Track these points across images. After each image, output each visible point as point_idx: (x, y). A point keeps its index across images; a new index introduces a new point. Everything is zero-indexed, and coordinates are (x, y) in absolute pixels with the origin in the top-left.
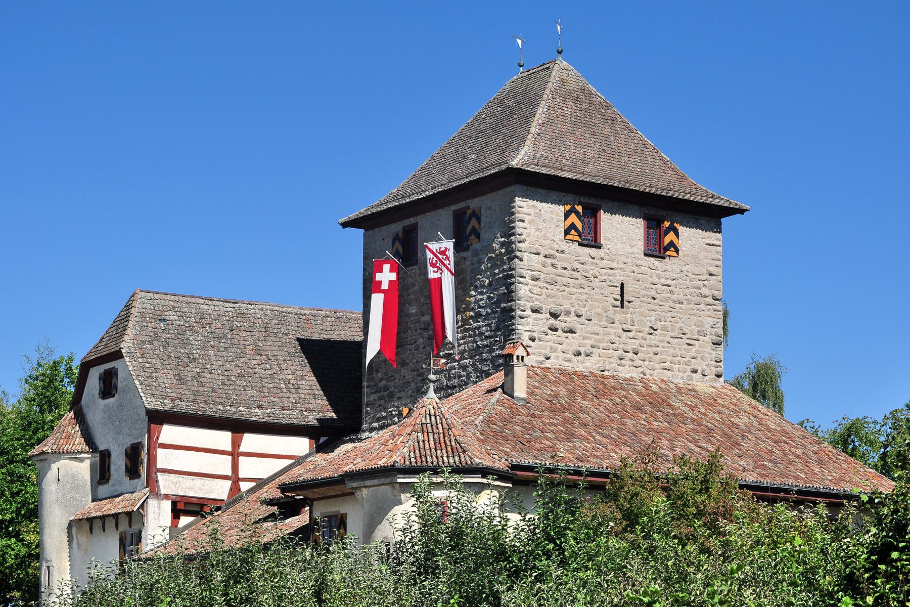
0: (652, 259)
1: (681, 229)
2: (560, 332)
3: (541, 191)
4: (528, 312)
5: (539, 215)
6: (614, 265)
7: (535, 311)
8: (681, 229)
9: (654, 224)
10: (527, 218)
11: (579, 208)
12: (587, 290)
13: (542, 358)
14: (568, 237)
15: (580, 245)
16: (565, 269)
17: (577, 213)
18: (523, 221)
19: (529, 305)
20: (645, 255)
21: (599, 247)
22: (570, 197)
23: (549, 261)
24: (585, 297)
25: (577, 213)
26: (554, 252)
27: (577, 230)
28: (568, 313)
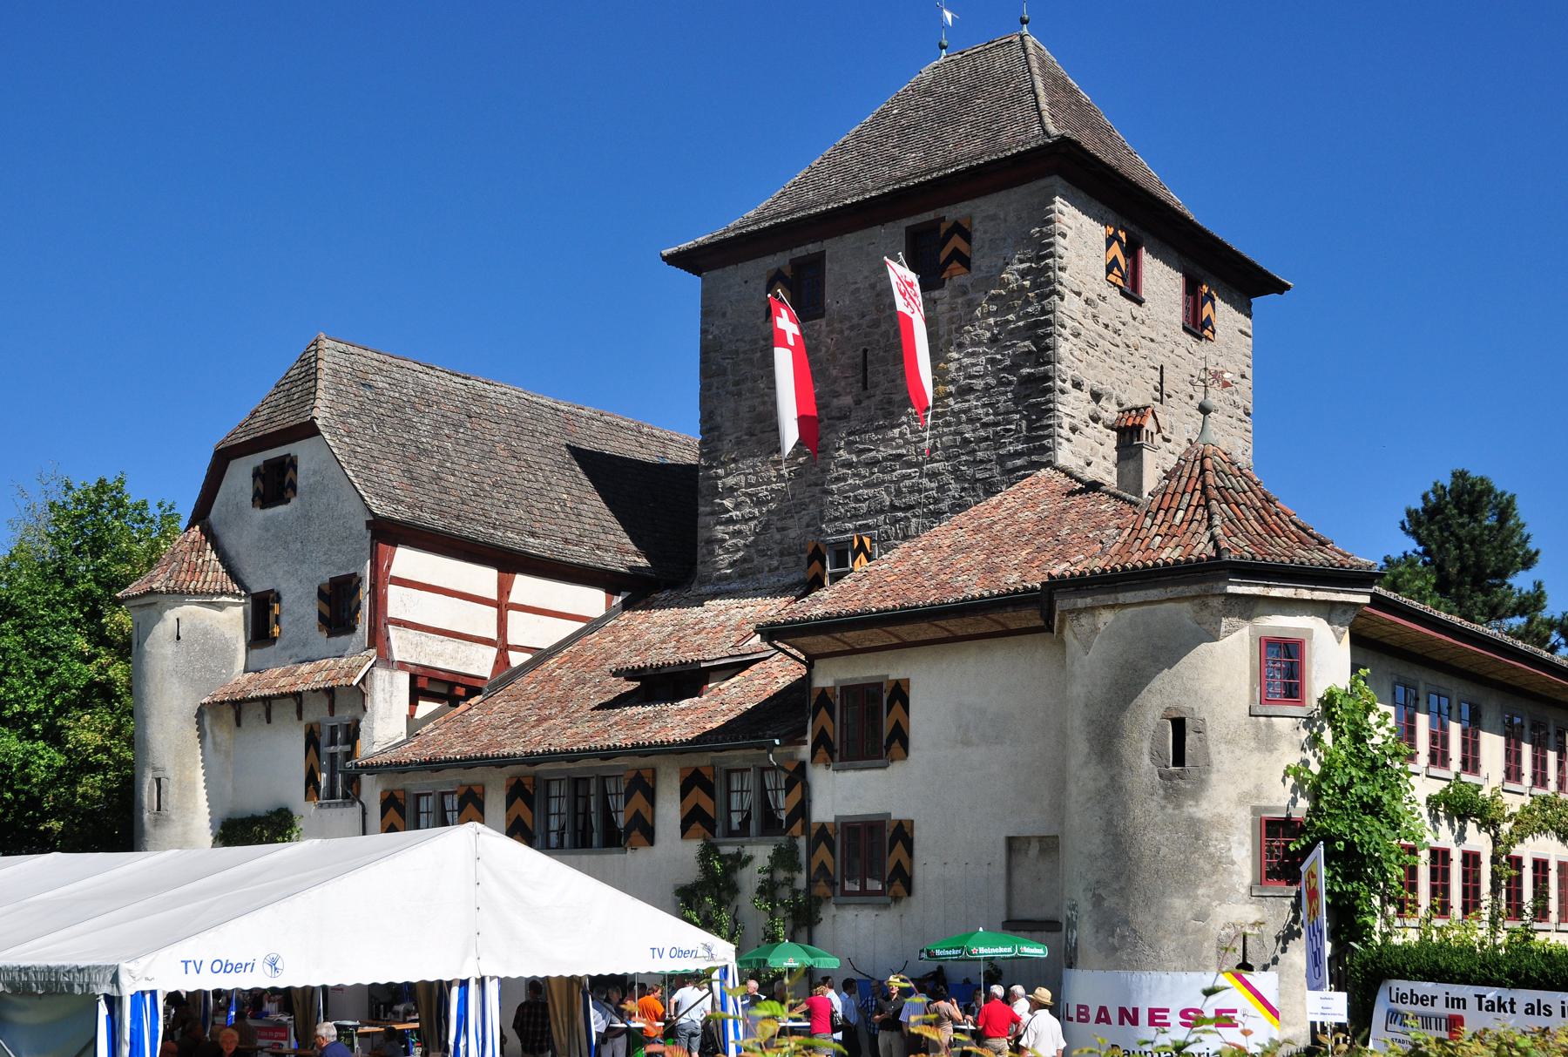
0: (1189, 337)
1: (1218, 301)
2: (1100, 426)
3: (1083, 195)
4: (1068, 385)
5: (1080, 234)
6: (1153, 336)
7: (1077, 385)
8: (1218, 301)
9: (1191, 287)
10: (1069, 233)
11: (1122, 235)
12: (1127, 366)
13: (1082, 463)
14: (1111, 277)
15: (1123, 293)
16: (1107, 326)
17: (1120, 241)
18: (1064, 236)
19: (1070, 373)
20: (1185, 329)
21: (1140, 302)
22: (1111, 216)
23: (1090, 310)
24: (1125, 377)
25: (1120, 241)
26: (1094, 297)
27: (1120, 269)
28: (1109, 399)
